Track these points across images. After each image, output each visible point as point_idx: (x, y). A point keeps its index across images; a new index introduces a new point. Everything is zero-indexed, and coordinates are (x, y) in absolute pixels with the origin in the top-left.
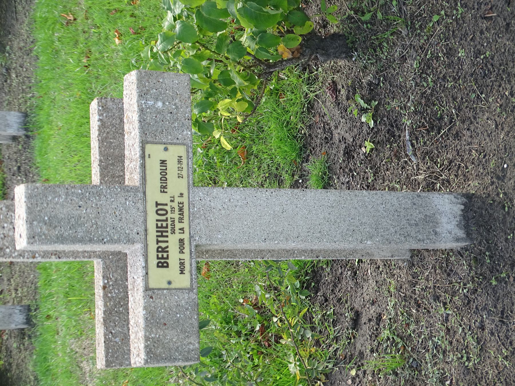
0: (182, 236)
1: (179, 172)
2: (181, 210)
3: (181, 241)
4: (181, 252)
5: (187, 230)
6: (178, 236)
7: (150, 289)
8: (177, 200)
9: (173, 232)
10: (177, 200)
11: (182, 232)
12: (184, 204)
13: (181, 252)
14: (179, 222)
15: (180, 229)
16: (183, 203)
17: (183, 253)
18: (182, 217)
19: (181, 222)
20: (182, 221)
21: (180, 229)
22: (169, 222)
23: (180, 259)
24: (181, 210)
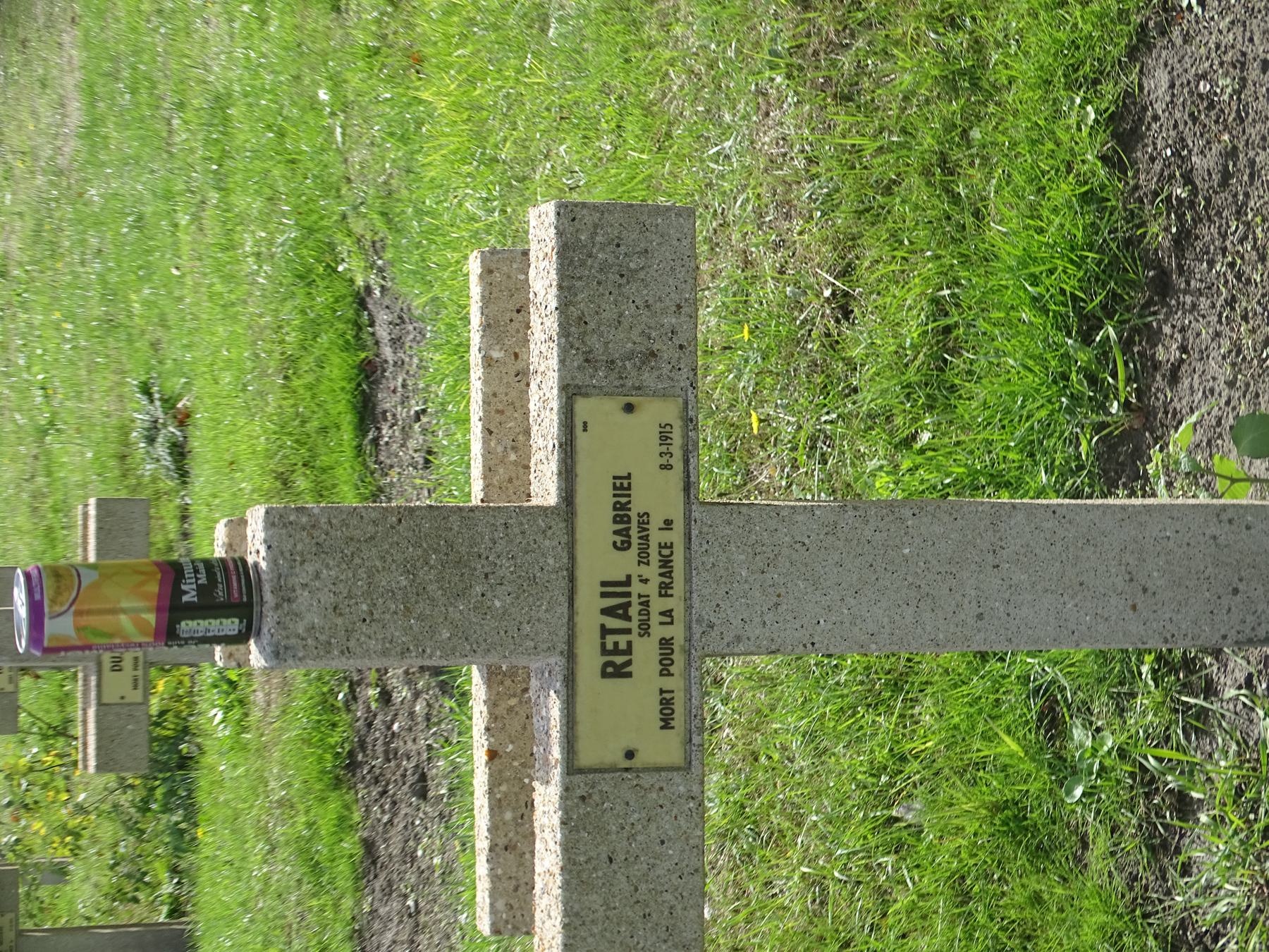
0: (667, 632)
2: (666, 563)
5: (679, 614)
6: (658, 631)
8: (656, 537)
11: (669, 620)
12: (674, 550)
13: (665, 672)
14: (661, 595)
15: (662, 614)
16: (671, 547)
18: (667, 581)
19: (666, 595)
20: (670, 592)
21: (662, 614)
23: (662, 692)
24: (666, 563)
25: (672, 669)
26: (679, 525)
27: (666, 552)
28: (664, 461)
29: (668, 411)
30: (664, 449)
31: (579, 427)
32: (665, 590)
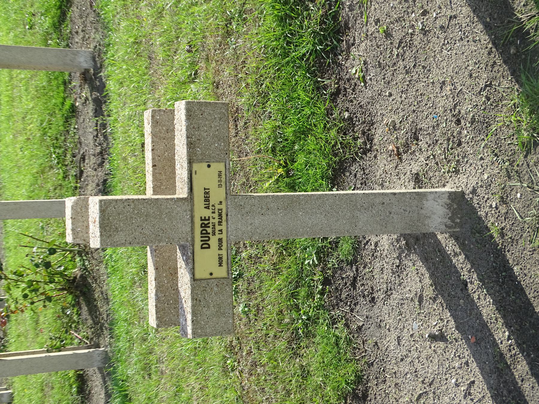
0: (220, 236)
1: (219, 183)
2: (220, 215)
3: (220, 240)
4: (220, 249)
5: (224, 232)
6: (218, 236)
8: (218, 207)
9: (214, 234)
10: (218, 207)
13: (220, 249)
15: (219, 231)
17: (221, 249)
19: (220, 225)
21: (219, 231)
22: (211, 227)
23: (219, 255)
24: (220, 215)
27: (220, 211)
28: (219, 183)
29: (221, 167)
30: (219, 179)
32: (220, 223)
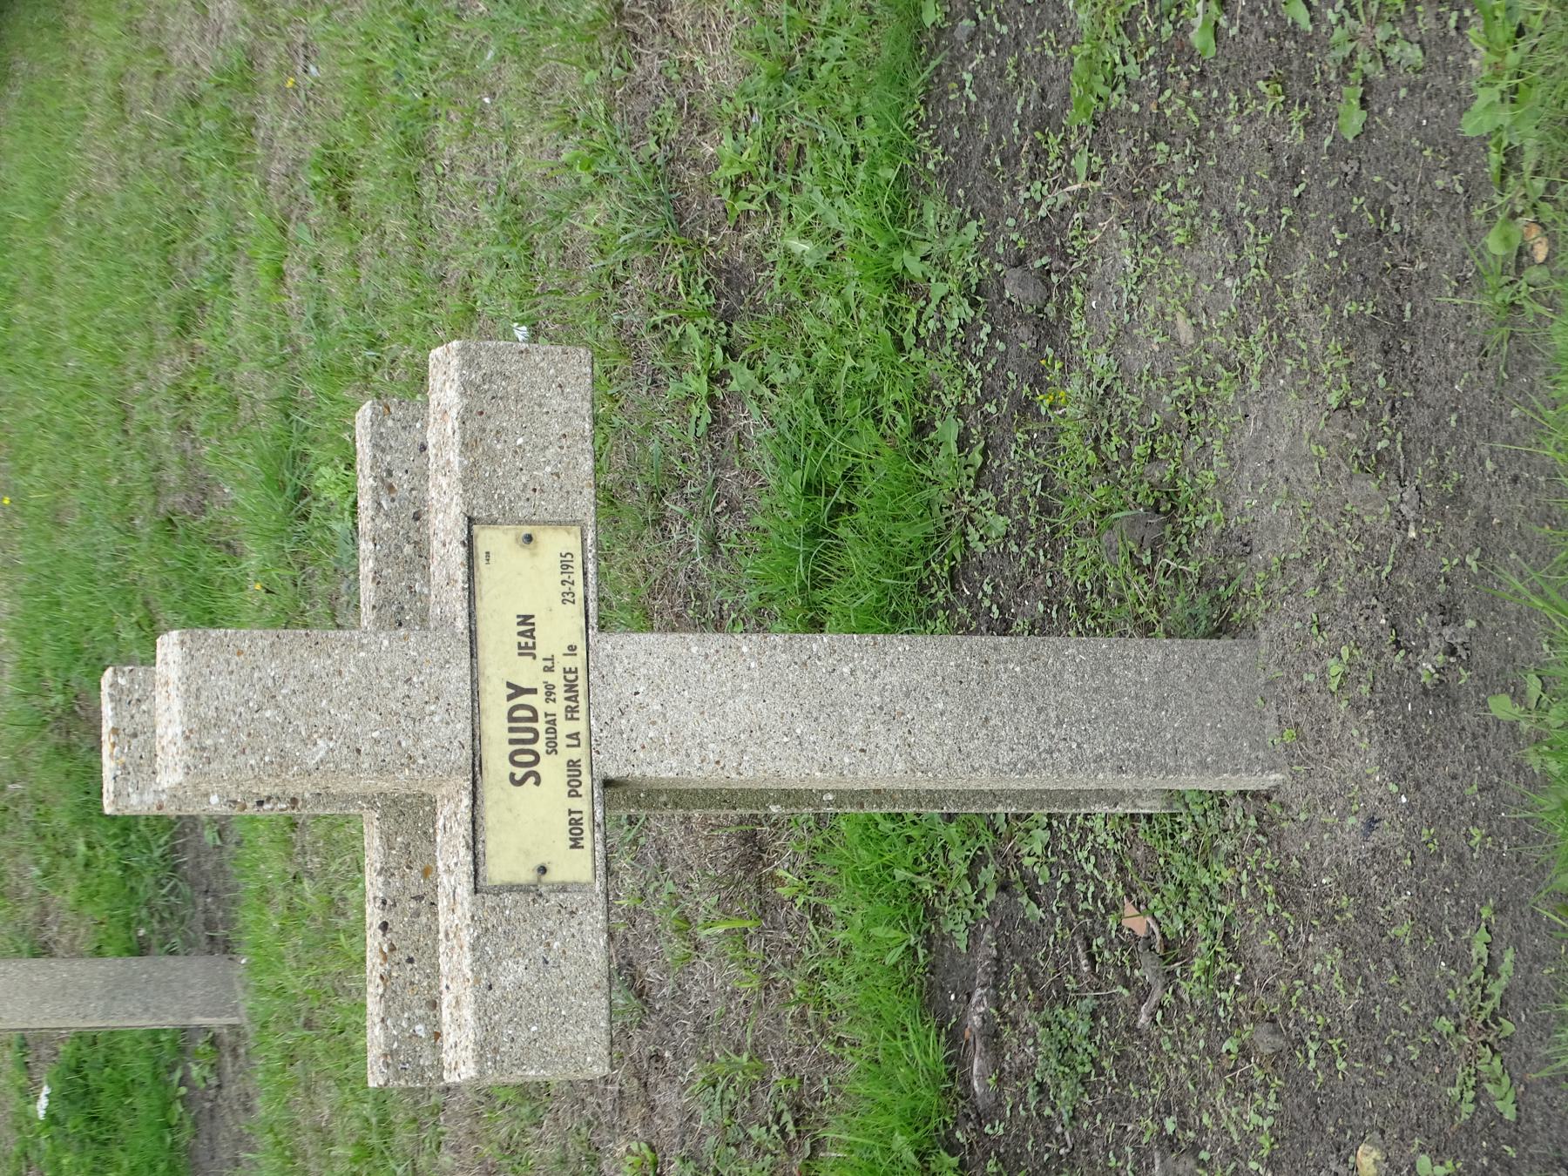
0: (575, 754)
5: (583, 737)
6: (566, 753)
7: (498, 890)
10: (563, 662)
13: (573, 793)
15: (569, 736)
19: (572, 718)
21: (569, 736)
23: (570, 812)
24: (571, 687)
25: (581, 790)
26: (581, 651)
27: (571, 677)
28: (566, 588)
30: (565, 577)
31: (482, 556)
32: (571, 713)
